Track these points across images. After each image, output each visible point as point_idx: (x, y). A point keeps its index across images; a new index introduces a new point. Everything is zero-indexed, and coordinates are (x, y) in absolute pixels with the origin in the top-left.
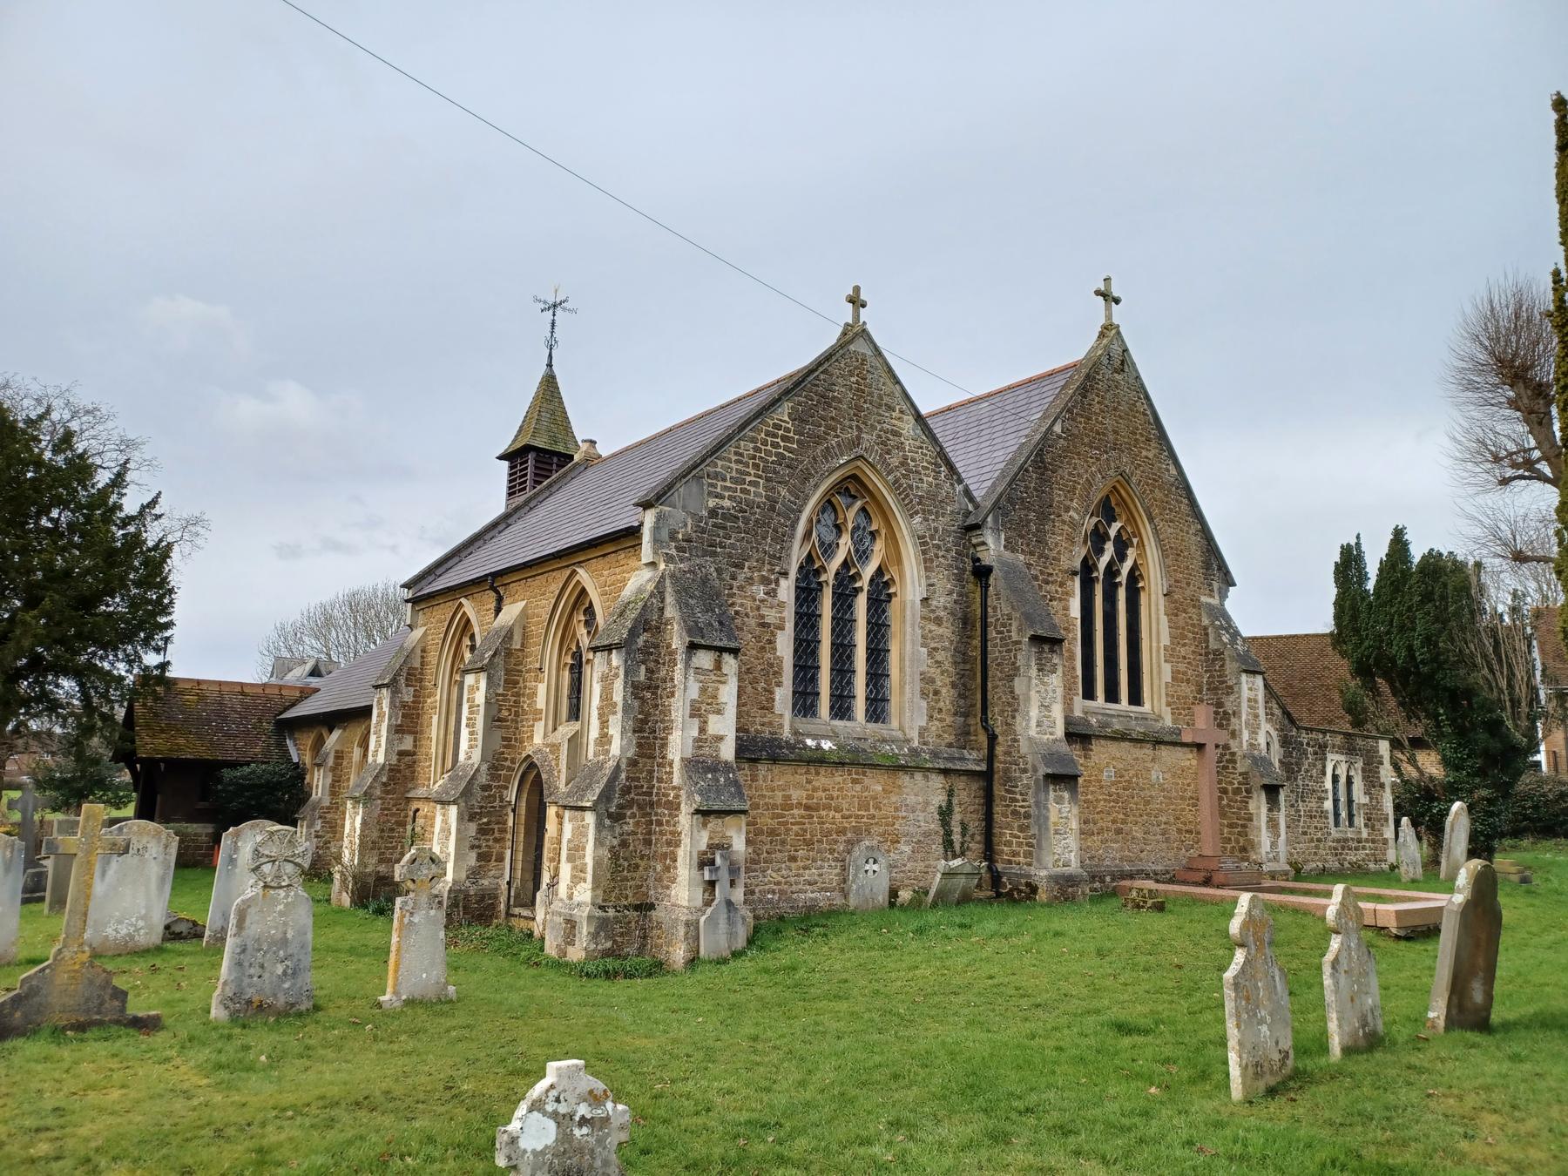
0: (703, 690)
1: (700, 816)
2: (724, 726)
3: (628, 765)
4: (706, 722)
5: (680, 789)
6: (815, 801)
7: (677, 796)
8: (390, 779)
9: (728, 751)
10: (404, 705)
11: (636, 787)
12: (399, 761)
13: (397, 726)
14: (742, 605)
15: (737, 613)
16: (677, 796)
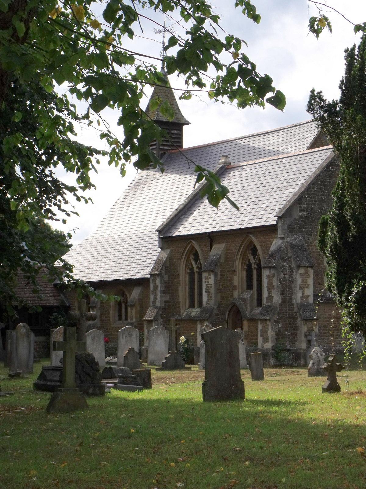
0: (303, 280)
1: (304, 321)
2: (309, 292)
3: (279, 305)
4: (304, 291)
5: (297, 313)
6: (339, 315)
7: (296, 315)
8: (163, 312)
9: (311, 300)
10: (165, 282)
11: (282, 312)
12: (165, 305)
13: (164, 291)
14: (312, 249)
15: (310, 251)
16: (296, 315)
